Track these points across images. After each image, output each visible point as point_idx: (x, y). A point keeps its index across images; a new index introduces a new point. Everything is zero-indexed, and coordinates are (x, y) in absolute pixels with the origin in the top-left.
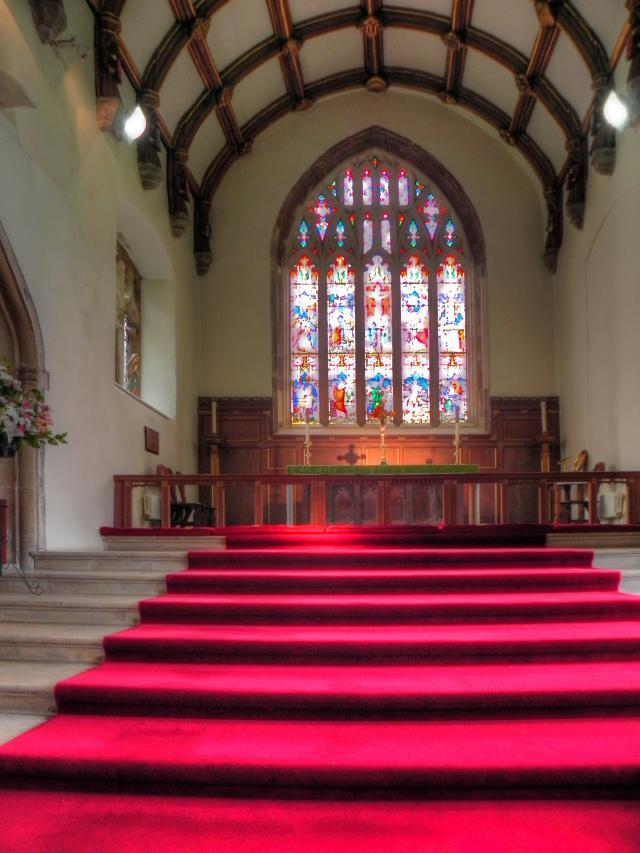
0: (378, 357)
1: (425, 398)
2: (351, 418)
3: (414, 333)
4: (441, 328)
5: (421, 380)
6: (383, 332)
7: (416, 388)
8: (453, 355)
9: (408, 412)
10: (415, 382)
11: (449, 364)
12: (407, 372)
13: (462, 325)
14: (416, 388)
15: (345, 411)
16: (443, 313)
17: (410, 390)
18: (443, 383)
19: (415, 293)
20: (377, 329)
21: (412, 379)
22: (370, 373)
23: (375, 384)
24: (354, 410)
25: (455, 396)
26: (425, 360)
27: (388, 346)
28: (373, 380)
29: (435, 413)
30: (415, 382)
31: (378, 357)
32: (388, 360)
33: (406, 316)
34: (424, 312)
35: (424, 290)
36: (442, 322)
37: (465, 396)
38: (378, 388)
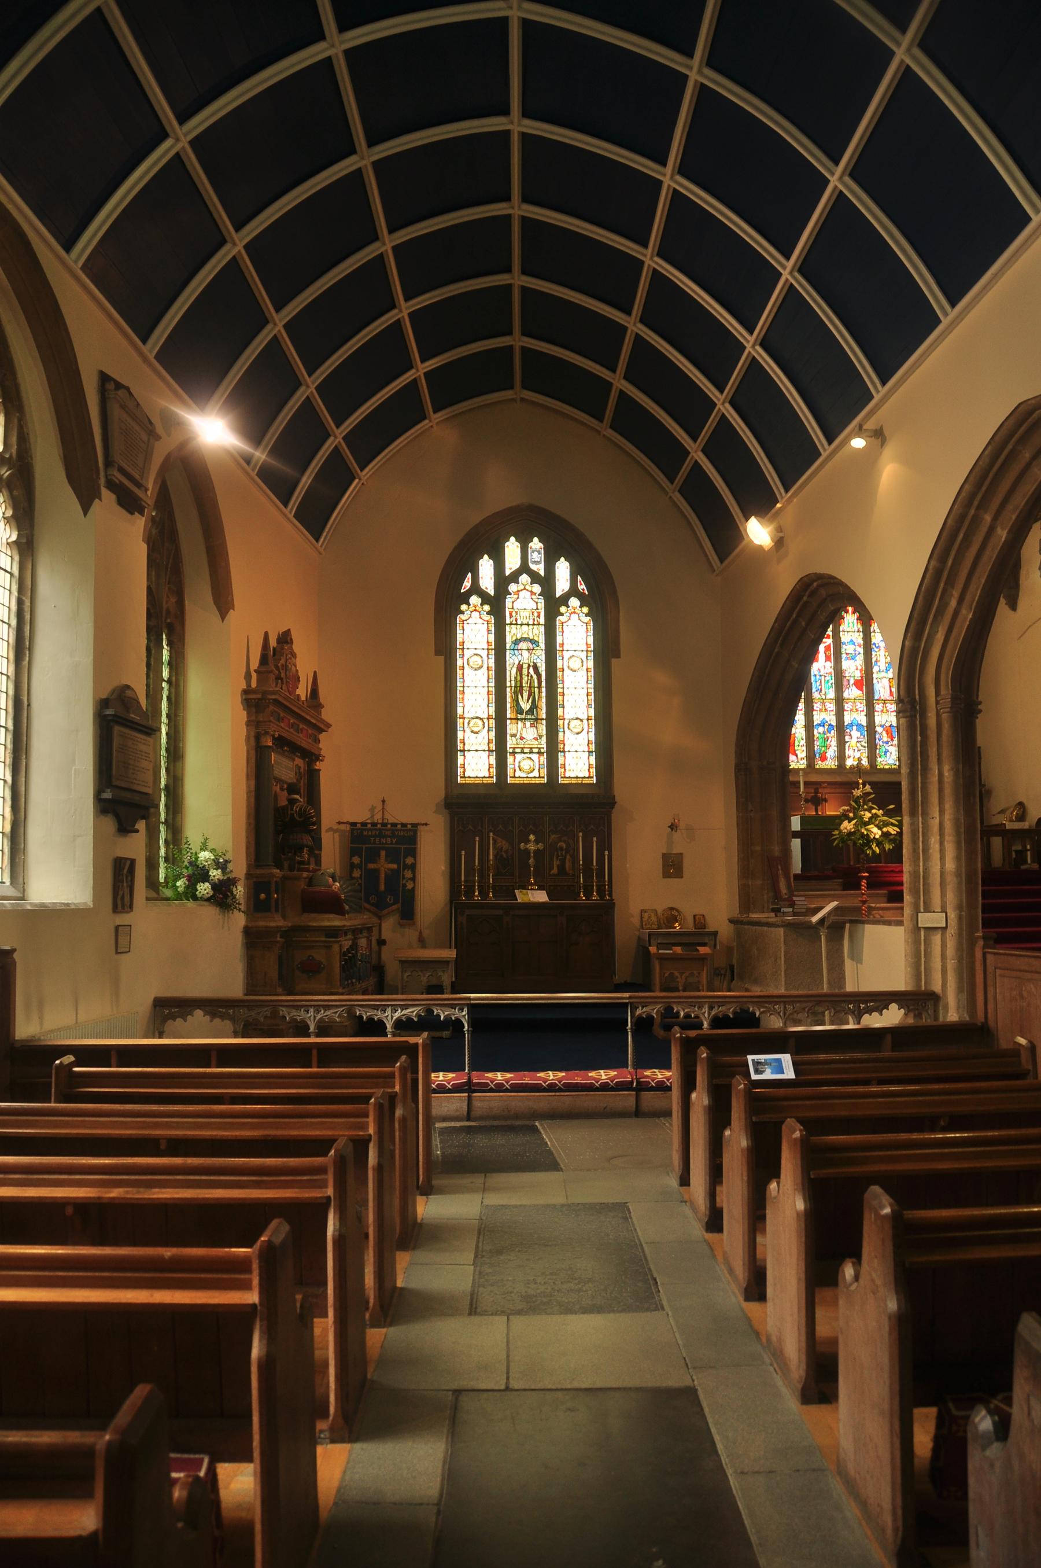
0: (823, 703)
1: (863, 744)
2: (802, 762)
3: (852, 681)
4: (875, 676)
5: (859, 726)
6: (827, 679)
7: (855, 734)
8: (885, 702)
9: (849, 757)
10: (855, 728)
11: (882, 711)
12: (847, 719)
13: (890, 675)
14: (855, 734)
15: (797, 756)
16: (877, 661)
17: (850, 735)
18: (879, 729)
19: (852, 640)
20: (821, 676)
21: (851, 725)
22: (817, 718)
23: (821, 729)
24: (804, 755)
25: (887, 743)
26: (862, 706)
27: (831, 694)
28: (820, 725)
29: (872, 757)
30: (855, 728)
31: (823, 703)
32: (831, 706)
33: (846, 664)
34: (860, 661)
35: (859, 638)
36: (875, 669)
37: (895, 742)
38: (824, 733)
